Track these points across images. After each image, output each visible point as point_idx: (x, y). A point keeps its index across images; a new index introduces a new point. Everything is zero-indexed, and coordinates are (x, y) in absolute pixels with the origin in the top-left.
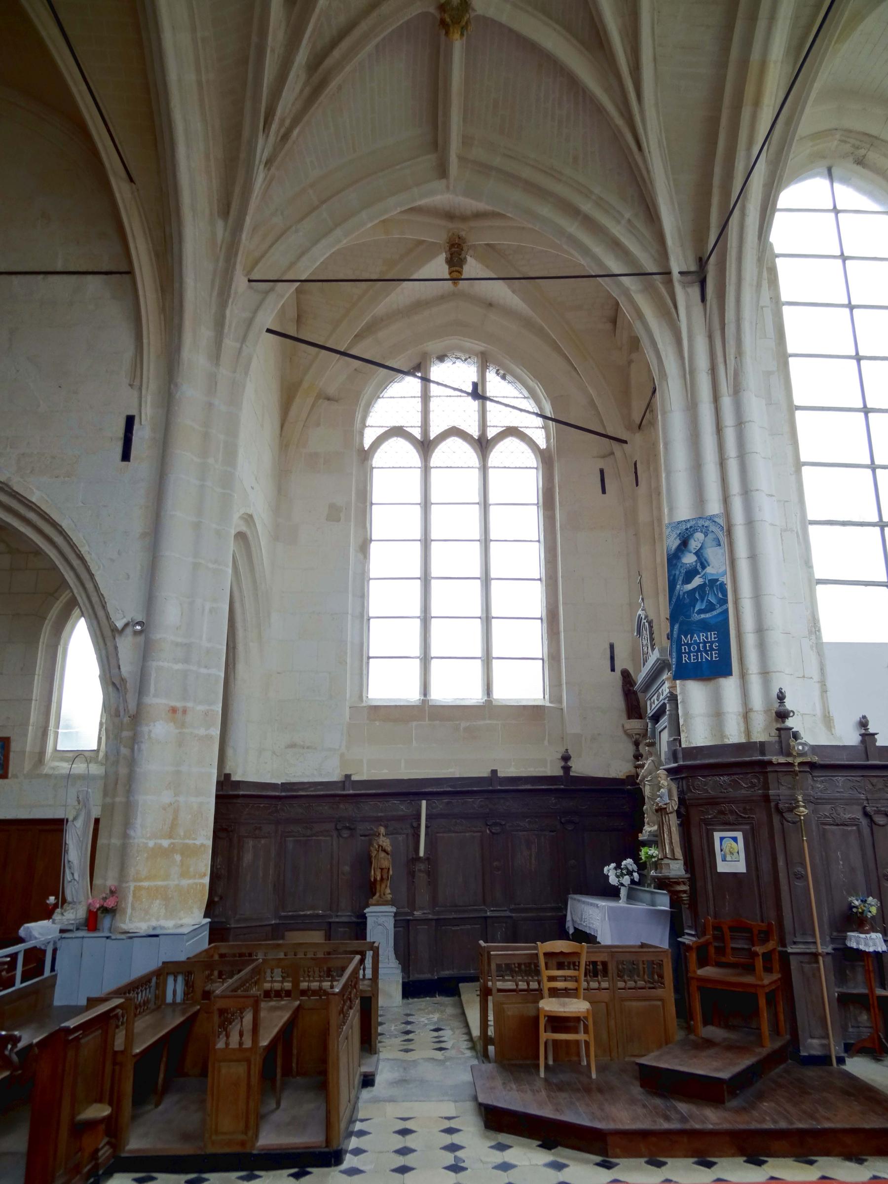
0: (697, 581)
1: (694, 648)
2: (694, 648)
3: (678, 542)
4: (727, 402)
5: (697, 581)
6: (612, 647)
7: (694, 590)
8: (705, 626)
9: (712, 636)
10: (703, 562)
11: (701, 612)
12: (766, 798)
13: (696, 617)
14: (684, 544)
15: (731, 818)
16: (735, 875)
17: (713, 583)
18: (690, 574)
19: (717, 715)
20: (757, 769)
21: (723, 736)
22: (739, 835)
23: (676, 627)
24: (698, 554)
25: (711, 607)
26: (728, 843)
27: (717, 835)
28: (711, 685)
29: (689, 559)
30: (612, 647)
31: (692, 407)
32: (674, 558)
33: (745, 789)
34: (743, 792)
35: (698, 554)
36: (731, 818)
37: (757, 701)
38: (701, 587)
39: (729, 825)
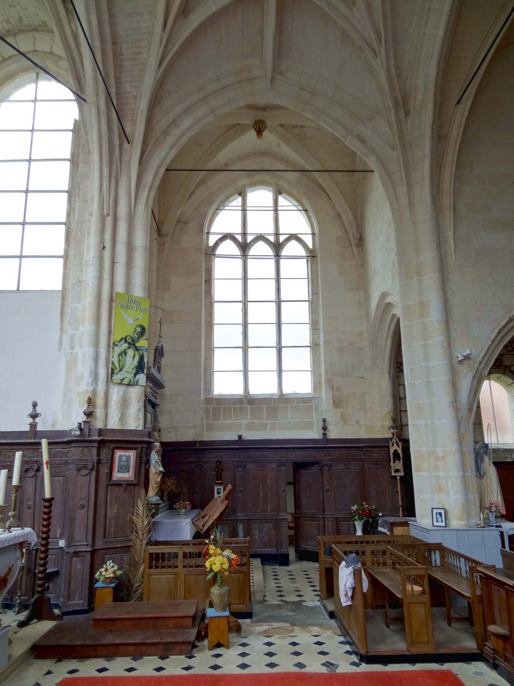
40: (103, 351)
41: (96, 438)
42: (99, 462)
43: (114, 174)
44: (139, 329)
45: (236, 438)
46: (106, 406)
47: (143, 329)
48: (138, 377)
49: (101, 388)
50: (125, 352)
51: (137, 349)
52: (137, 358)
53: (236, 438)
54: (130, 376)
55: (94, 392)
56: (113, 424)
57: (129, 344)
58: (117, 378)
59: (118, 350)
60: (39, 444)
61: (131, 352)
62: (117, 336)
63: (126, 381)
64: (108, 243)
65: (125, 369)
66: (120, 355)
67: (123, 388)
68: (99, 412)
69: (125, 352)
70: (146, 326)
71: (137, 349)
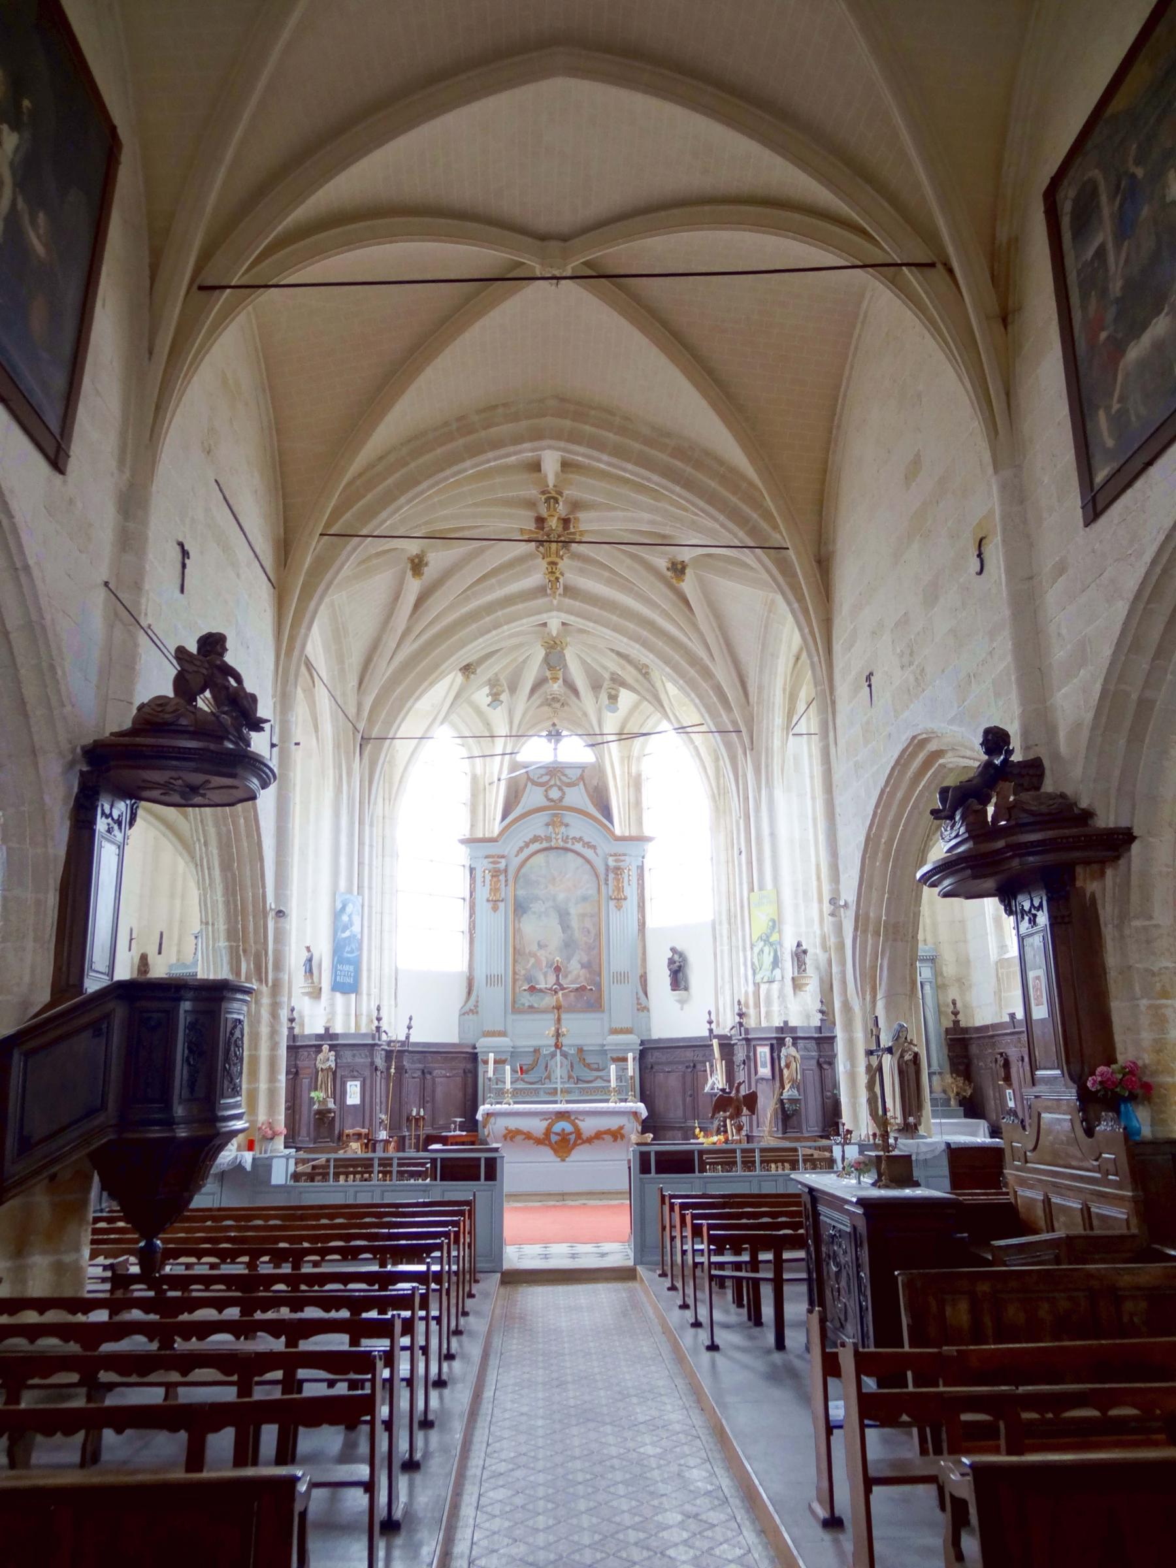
0: (347, 934)
1: (343, 973)
2: (343, 973)
3: (339, 906)
4: (367, 828)
5: (347, 934)
6: (131, 930)
7: (346, 938)
8: (349, 962)
9: (352, 968)
10: (351, 923)
11: (348, 952)
12: (372, 1063)
13: (346, 955)
14: (344, 908)
15: (356, 1074)
16: (354, 1106)
17: (353, 936)
18: (345, 928)
19: (347, 1015)
20: (369, 1048)
21: (349, 1027)
22: (358, 1083)
23: (336, 959)
24: (350, 916)
25: (352, 952)
26: (354, 1088)
27: (349, 1084)
28: (346, 996)
29: (345, 918)
30: (131, 930)
31: (352, 824)
32: (337, 915)
33: (361, 1060)
34: (362, 1060)
35: (350, 916)
36: (356, 1074)
37: (364, 1011)
38: (349, 938)
39: (354, 1078)
40: (749, 953)
41: (743, 1036)
42: (748, 1057)
43: (740, 773)
44: (771, 924)
45: (1007, 1019)
46: (757, 1005)
47: (773, 921)
48: (774, 972)
49: (751, 988)
50: (762, 951)
51: (771, 944)
52: (772, 954)
53: (1007, 1019)
54: (768, 973)
55: (746, 993)
56: (764, 1024)
57: (765, 941)
58: (758, 978)
59: (756, 950)
60: (712, 1045)
61: (766, 949)
62: (755, 938)
63: (765, 980)
64: (743, 849)
65: (764, 967)
66: (759, 954)
67: (767, 985)
68: (752, 1011)
69: (762, 951)
70: (776, 918)
71: (771, 944)
